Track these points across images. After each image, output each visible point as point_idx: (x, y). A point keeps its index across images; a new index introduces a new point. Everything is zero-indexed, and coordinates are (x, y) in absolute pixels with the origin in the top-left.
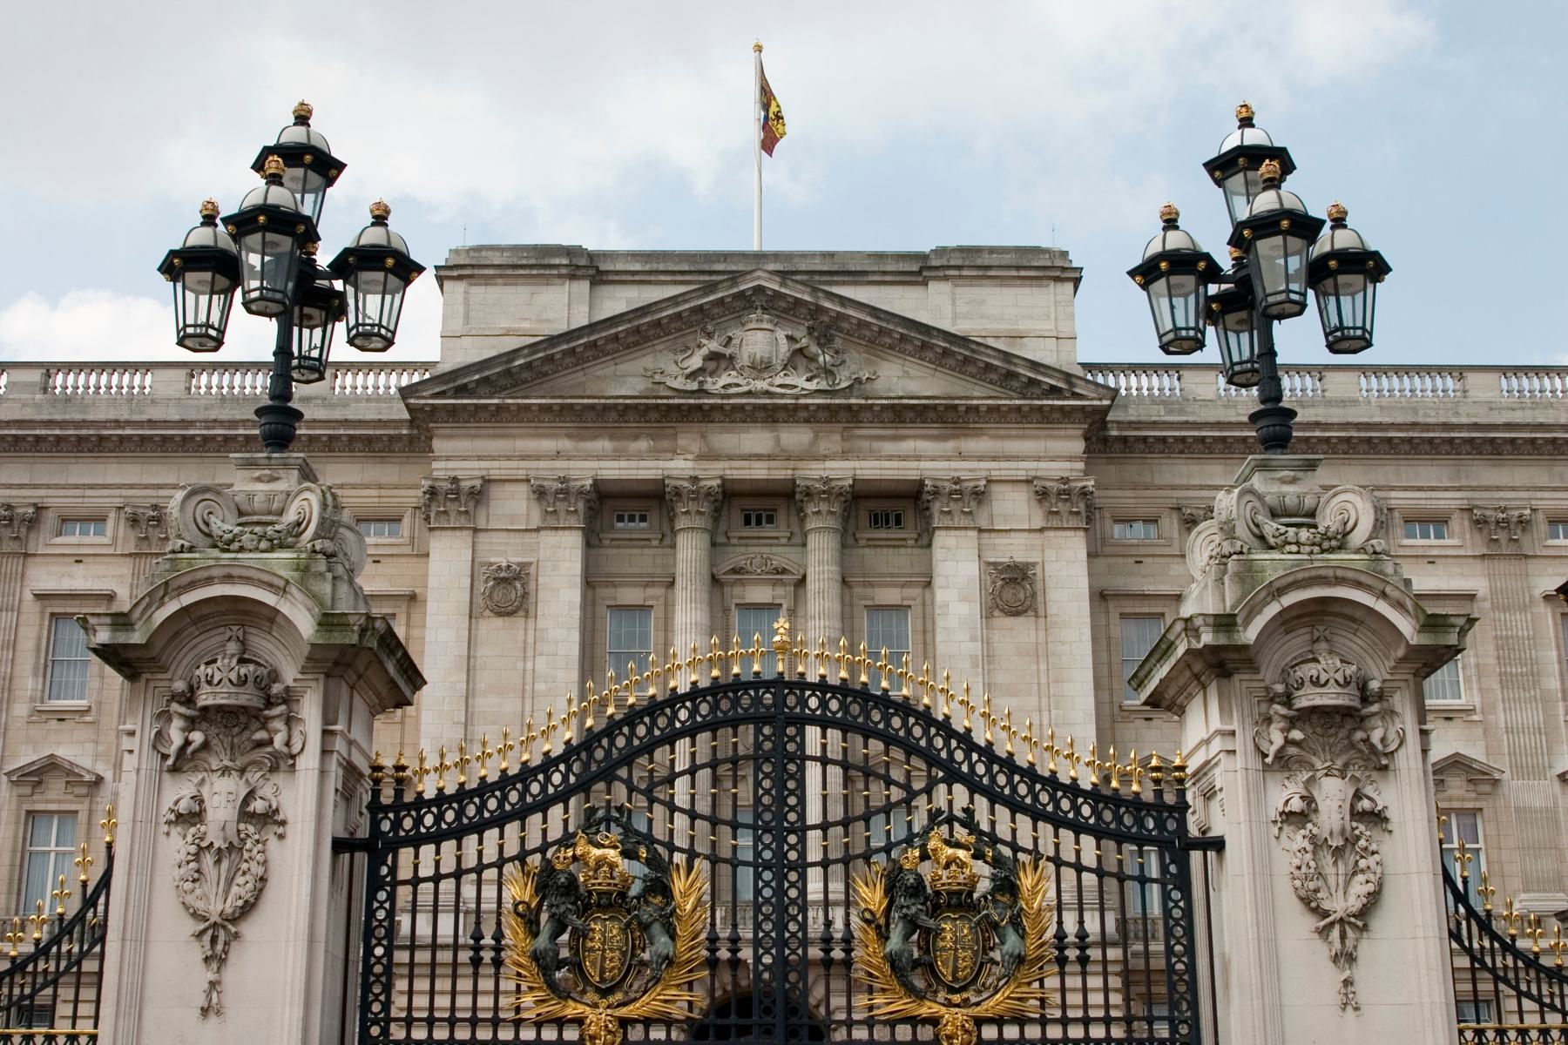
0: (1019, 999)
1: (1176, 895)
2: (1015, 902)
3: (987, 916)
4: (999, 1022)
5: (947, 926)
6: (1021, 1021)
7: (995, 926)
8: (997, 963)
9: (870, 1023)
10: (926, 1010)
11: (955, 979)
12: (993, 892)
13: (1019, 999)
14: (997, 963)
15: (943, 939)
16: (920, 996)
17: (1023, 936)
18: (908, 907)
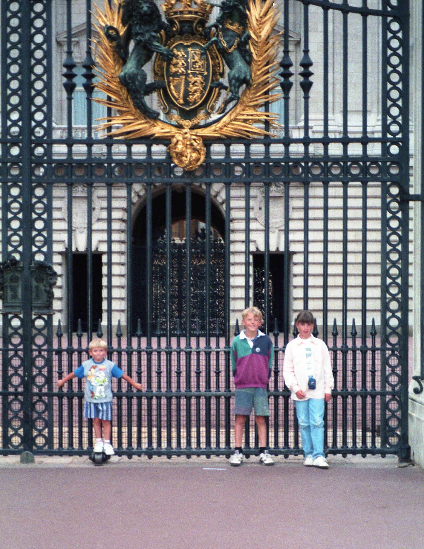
0: (245, 121)
1: (395, 26)
2: (244, 32)
3: (216, 43)
4: (228, 141)
5: (180, 53)
6: (247, 141)
7: (223, 52)
8: (225, 88)
9: (109, 142)
10: (158, 130)
11: (187, 103)
12: (221, 21)
13: (245, 121)
14: (225, 88)
15: (175, 65)
16: (151, 116)
17: (249, 62)
18: (142, 34)
